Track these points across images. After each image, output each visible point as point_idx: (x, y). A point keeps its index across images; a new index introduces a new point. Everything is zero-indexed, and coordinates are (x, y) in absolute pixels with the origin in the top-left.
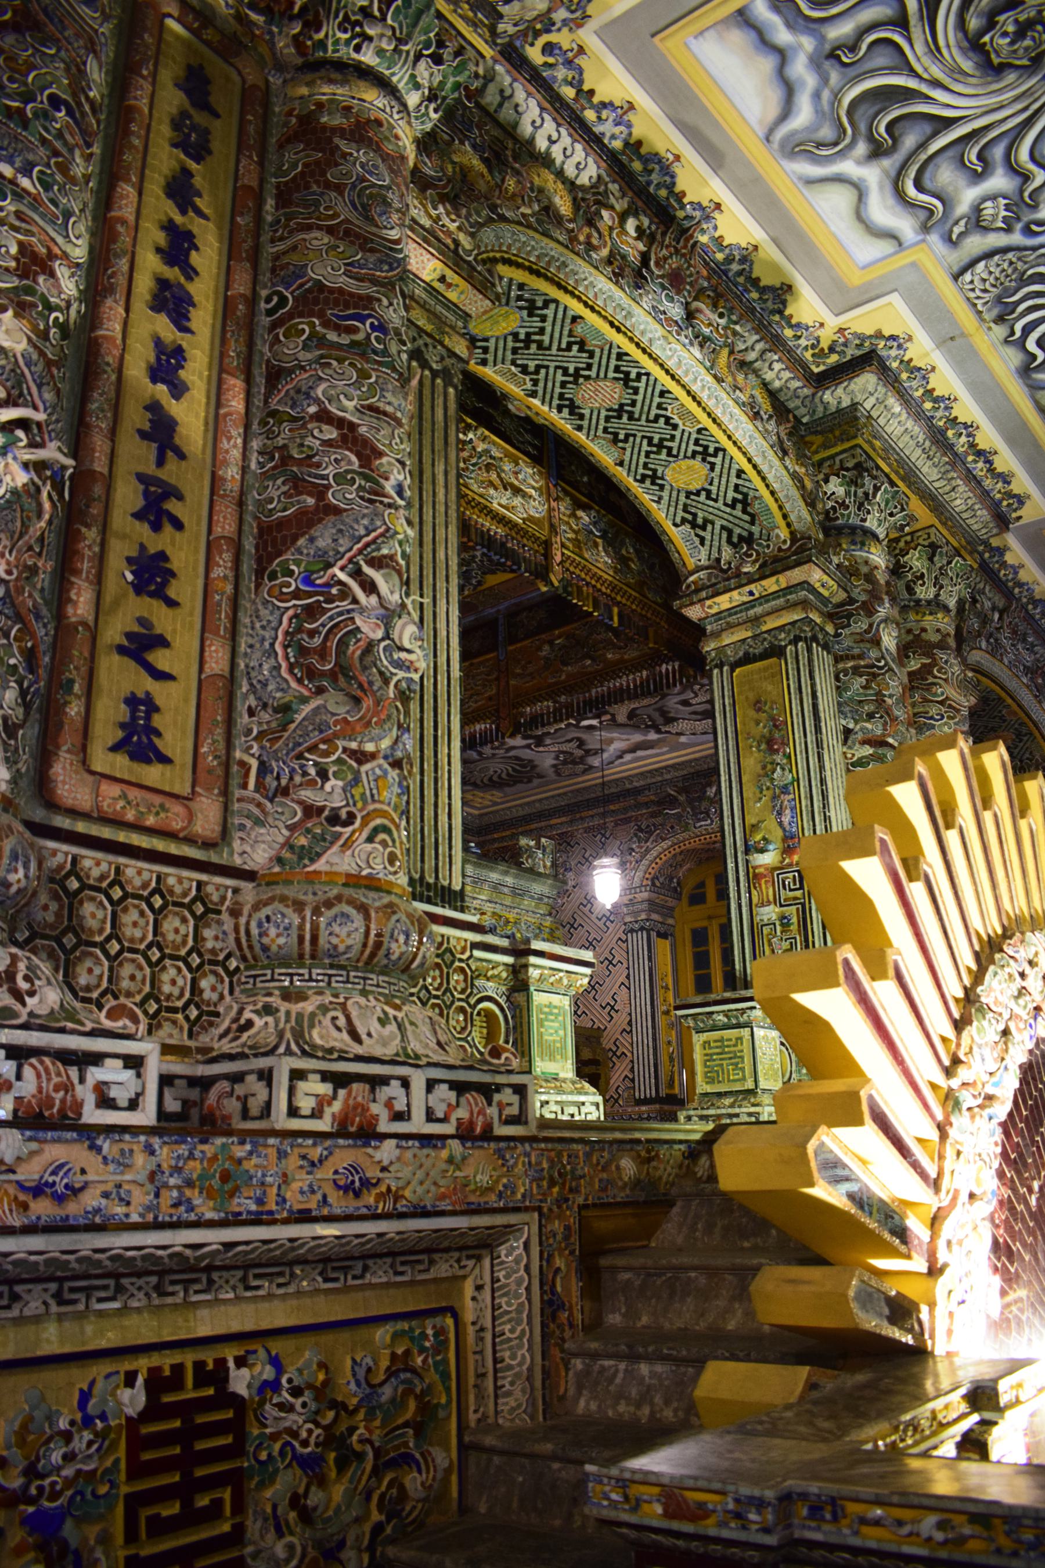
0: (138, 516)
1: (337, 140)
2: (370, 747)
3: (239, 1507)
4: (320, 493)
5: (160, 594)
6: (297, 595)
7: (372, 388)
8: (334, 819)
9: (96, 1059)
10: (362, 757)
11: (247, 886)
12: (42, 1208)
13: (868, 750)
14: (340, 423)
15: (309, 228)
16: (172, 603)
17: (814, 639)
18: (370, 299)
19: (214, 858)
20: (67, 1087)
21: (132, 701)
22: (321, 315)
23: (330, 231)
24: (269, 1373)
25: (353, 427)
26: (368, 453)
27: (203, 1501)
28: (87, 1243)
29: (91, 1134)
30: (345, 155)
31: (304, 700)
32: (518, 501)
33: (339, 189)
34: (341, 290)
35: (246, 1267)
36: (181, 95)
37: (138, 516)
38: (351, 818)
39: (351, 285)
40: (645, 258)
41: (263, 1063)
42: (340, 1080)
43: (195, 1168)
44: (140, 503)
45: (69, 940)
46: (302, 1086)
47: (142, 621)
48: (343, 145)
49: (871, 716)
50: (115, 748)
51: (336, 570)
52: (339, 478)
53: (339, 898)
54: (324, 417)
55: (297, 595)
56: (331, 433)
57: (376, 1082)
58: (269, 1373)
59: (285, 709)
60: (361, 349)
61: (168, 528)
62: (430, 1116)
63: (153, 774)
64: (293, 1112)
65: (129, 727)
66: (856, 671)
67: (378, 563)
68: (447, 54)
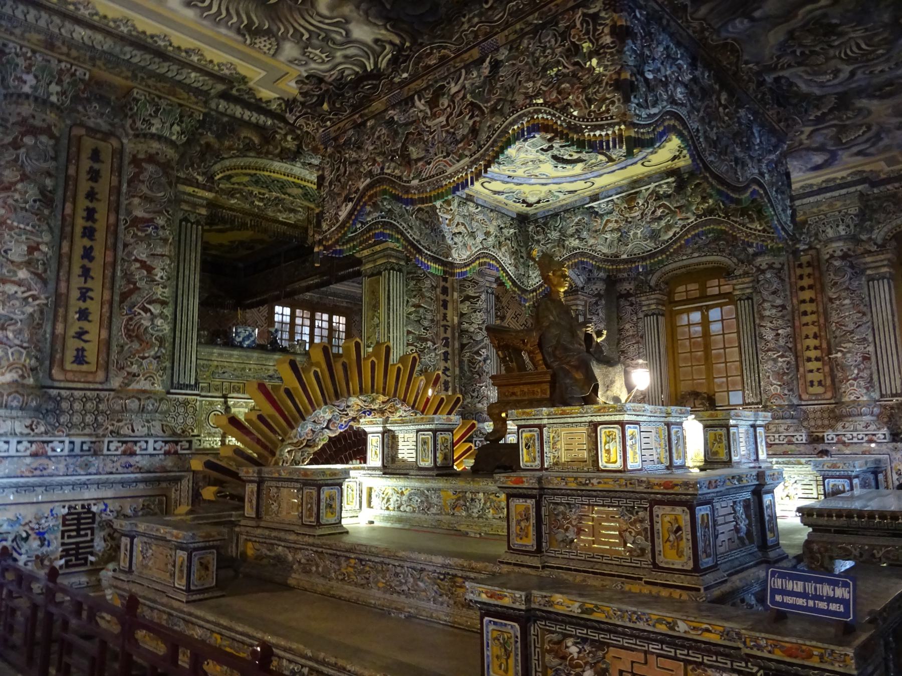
0: (79, 299)
1: (144, 164)
2: (146, 355)
3: (92, 534)
4: (135, 284)
5: (86, 319)
6: (127, 314)
7: (151, 249)
8: (134, 375)
9: (51, 442)
10: (144, 358)
11: (112, 393)
12: (38, 472)
13: (413, 309)
14: (141, 262)
15: (134, 196)
16: (90, 321)
17: (393, 269)
18: (153, 219)
19: (105, 387)
20: (44, 448)
21: (78, 350)
22: (137, 227)
23: (141, 197)
24: (104, 507)
25: (145, 262)
26: (150, 269)
27: (82, 533)
28: (48, 479)
29: (49, 457)
30: (146, 169)
31: (127, 344)
32: (292, 215)
33: (143, 182)
34: (143, 218)
35: (98, 484)
36: (89, 161)
37: (79, 299)
38: (139, 375)
39: (147, 216)
40: (299, 147)
41: (102, 439)
42: (123, 442)
43: (78, 463)
44: (79, 295)
45: (58, 412)
46: (111, 444)
47: (80, 328)
48: (144, 164)
49: (415, 296)
50: (73, 362)
51: (136, 309)
52: (140, 279)
53: (133, 397)
54: (136, 260)
55: (127, 314)
56: (138, 265)
57: (135, 443)
58: (104, 507)
59: (122, 347)
60: (149, 236)
61: (88, 301)
62: (155, 449)
63: (84, 367)
64: (108, 450)
65: (77, 357)
66: (413, 278)
67: (150, 303)
68: (185, 119)
